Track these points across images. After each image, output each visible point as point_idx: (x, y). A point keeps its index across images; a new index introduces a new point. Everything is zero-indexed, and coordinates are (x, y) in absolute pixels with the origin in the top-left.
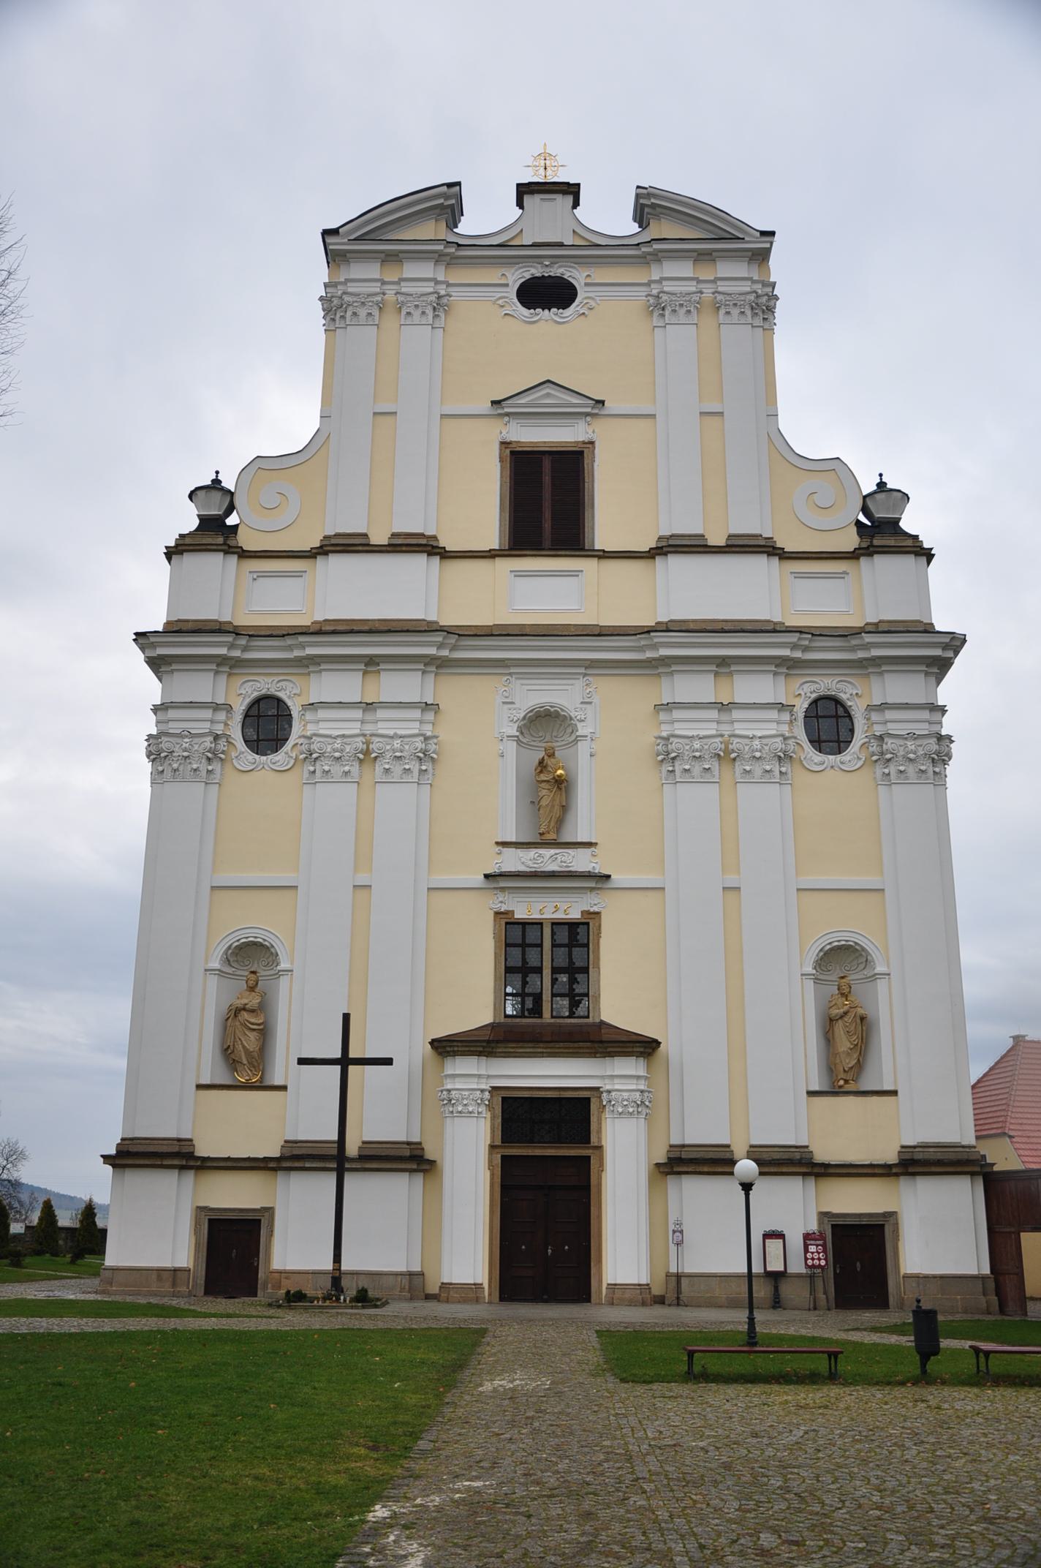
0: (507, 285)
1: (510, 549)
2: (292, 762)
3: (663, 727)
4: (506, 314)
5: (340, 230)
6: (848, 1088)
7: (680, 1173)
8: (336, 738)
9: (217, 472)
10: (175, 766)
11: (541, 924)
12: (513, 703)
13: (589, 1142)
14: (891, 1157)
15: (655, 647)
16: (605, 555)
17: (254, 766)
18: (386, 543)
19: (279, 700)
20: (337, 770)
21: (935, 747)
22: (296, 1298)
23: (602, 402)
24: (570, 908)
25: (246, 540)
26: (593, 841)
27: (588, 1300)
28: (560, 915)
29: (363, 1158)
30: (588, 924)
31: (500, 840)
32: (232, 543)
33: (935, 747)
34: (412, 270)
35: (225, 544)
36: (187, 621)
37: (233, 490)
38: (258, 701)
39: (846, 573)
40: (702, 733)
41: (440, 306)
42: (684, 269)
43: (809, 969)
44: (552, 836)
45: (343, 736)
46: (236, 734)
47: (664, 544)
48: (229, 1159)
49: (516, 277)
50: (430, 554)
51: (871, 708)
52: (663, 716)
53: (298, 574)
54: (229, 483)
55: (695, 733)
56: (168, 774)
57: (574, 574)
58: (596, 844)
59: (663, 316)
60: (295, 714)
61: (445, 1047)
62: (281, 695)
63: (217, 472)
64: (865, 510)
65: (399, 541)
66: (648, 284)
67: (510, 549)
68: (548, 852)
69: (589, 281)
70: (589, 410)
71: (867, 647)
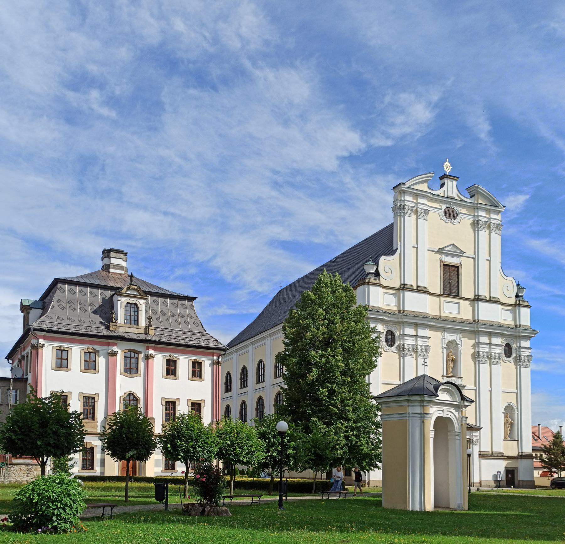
0: (441, 209)
1: (443, 294)
4: (442, 219)
17: (388, 351)
23: (464, 253)
26: (462, 376)
49: (444, 207)
50: (428, 293)
58: (462, 377)
67: (443, 294)
69: (460, 211)
70: (461, 254)
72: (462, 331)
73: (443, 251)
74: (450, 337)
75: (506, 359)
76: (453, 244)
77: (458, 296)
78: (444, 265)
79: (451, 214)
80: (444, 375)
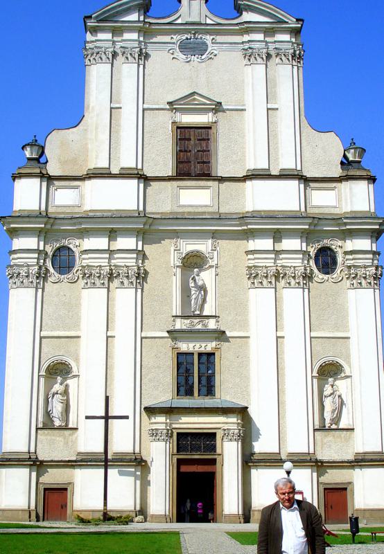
0: (174, 43)
2: (76, 278)
3: (250, 261)
5: (93, 16)
6: (334, 426)
7: (256, 466)
8: (97, 267)
9: (35, 136)
10: (21, 280)
11: (193, 354)
12: (180, 250)
13: (215, 452)
14: (351, 457)
15: (247, 224)
16: (222, 180)
18: (118, 173)
19: (69, 248)
20: (98, 282)
21: (374, 271)
22: (83, 521)
23: (221, 103)
24: (209, 346)
25: (53, 169)
27: (214, 520)
28: (203, 350)
29: (113, 460)
30: (214, 354)
31: (174, 314)
32: (44, 172)
33: (374, 271)
34: (127, 36)
35: (41, 173)
36: (25, 210)
37: (43, 145)
38: (59, 249)
39: (335, 187)
40: (268, 265)
41: (144, 56)
42: (260, 37)
43: (315, 374)
44: (198, 312)
45: (100, 266)
46: (49, 264)
47: (250, 174)
48: (52, 461)
51: (346, 253)
52: (250, 256)
53: (77, 187)
54: (40, 142)
55: (264, 264)
56: (18, 283)
57: (208, 188)
59: (249, 60)
60: (77, 255)
61: (151, 411)
62: (71, 246)
63: (35, 136)
64: (345, 156)
65: (124, 172)
66: (243, 43)
68: (196, 321)
71: (346, 224)
72: (215, 235)
73: (175, 106)
74: (188, 246)
75: (321, 276)
76: (194, 92)
77: (209, 175)
78: (178, 128)
79: (193, 48)
80: (178, 314)
